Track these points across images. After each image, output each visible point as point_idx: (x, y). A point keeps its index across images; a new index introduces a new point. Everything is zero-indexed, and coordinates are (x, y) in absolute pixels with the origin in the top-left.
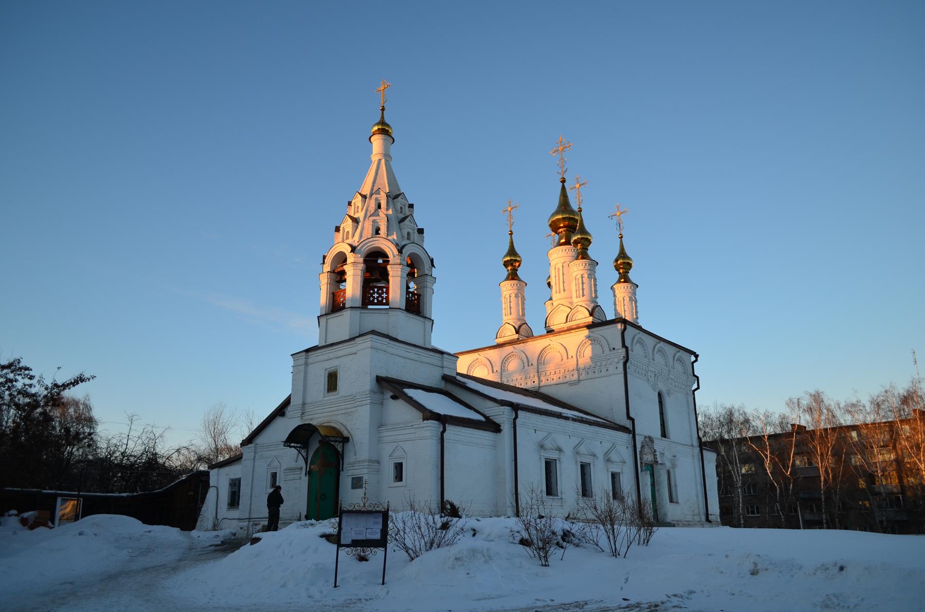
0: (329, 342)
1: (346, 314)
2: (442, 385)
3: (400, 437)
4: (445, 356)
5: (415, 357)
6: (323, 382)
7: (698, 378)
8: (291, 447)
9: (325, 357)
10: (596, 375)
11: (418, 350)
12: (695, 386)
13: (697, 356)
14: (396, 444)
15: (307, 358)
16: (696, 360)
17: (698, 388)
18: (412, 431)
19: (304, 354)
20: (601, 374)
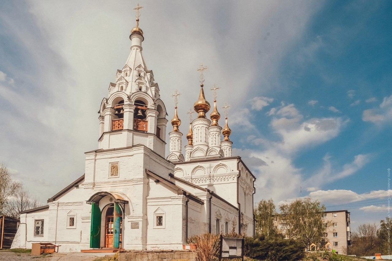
0: (111, 148)
1: (125, 133)
2: (169, 178)
3: (160, 203)
4: (170, 163)
5: (159, 162)
6: (108, 169)
7: (255, 188)
8: (91, 204)
9: (110, 156)
10: (223, 182)
11: (161, 158)
12: (253, 192)
13: (255, 179)
14: (158, 206)
15: (96, 156)
16: (255, 181)
17: (255, 193)
18: (170, 200)
19: (94, 153)
20: (224, 182)
